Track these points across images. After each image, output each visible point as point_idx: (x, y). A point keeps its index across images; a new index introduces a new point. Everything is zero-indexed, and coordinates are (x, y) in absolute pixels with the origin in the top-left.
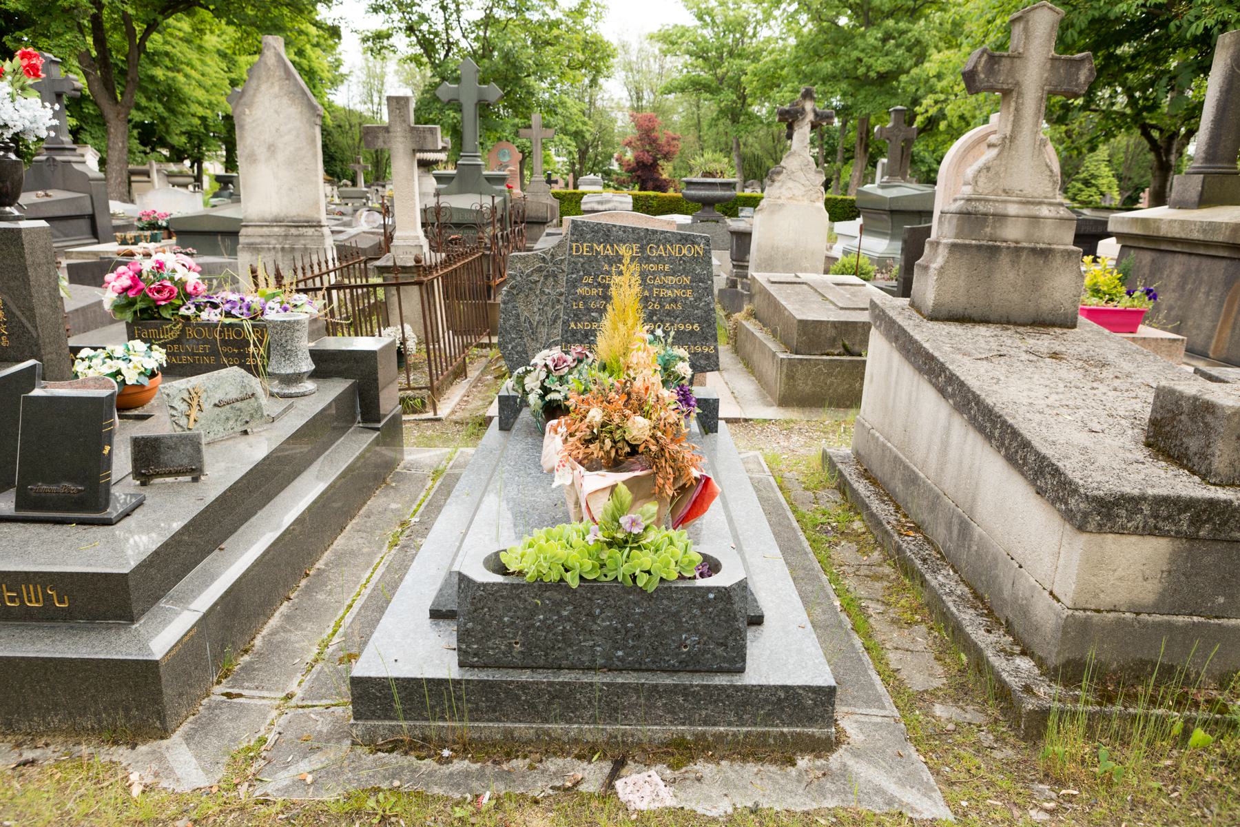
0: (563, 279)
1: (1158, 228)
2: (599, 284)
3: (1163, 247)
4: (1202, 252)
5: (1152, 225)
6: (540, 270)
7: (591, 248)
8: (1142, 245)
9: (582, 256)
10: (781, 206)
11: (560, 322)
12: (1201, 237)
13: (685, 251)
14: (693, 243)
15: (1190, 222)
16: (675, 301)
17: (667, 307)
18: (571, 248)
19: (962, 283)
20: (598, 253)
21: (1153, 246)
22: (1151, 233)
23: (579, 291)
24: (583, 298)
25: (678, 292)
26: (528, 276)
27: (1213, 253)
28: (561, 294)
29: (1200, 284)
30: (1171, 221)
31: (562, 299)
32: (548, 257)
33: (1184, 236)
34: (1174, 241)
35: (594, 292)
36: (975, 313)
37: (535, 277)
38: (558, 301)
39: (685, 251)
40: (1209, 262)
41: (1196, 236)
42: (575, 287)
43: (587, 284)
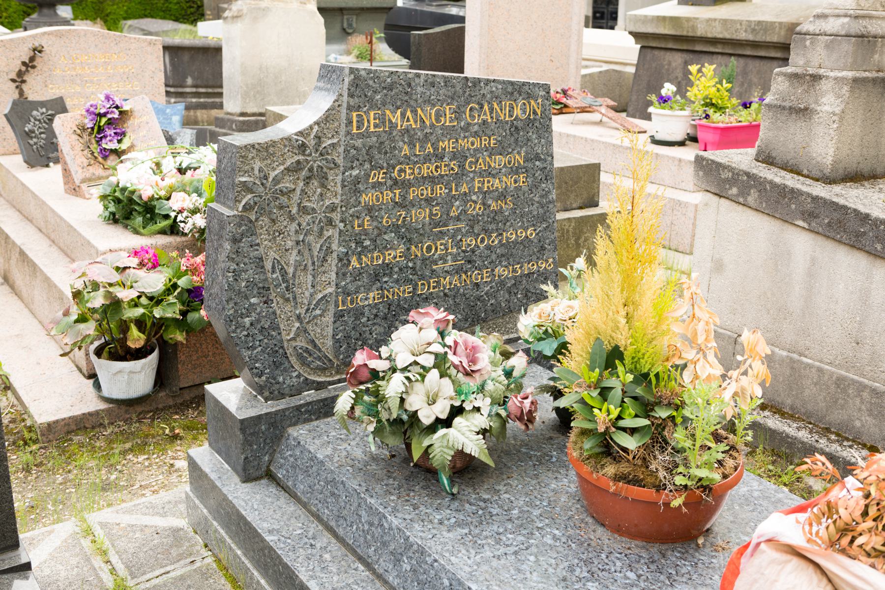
0: (336, 179)
1: (694, 28)
2: (396, 182)
3: (698, 48)
4: (748, 53)
5: (686, 25)
6: (297, 167)
7: (382, 120)
8: (670, 45)
9: (367, 135)
10: (266, 10)
11: (333, 260)
12: (751, 37)
13: (517, 112)
14: (529, 96)
15: (733, 22)
16: (502, 196)
17: (494, 206)
18: (350, 122)
19: (858, 130)
20: (393, 126)
21: (685, 48)
22: (685, 33)
23: (364, 198)
24: (370, 210)
25: (509, 181)
26: (276, 181)
27: (762, 53)
28: (333, 208)
29: (750, 87)
30: (708, 20)
31: (336, 216)
32: (311, 142)
33: (728, 36)
34: (714, 41)
35: (388, 195)
36: (865, 168)
37: (286, 184)
38: (330, 222)
39: (517, 112)
40: (757, 63)
41: (743, 36)
42: (357, 192)
43: (377, 185)
